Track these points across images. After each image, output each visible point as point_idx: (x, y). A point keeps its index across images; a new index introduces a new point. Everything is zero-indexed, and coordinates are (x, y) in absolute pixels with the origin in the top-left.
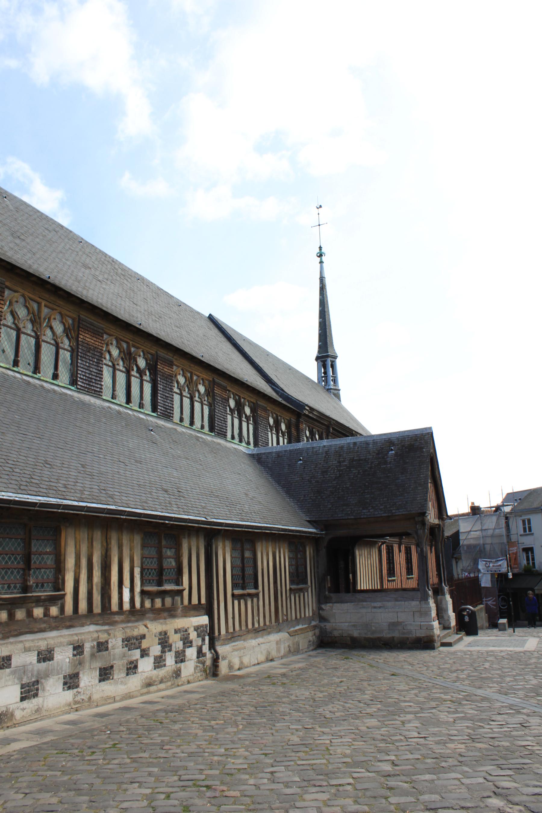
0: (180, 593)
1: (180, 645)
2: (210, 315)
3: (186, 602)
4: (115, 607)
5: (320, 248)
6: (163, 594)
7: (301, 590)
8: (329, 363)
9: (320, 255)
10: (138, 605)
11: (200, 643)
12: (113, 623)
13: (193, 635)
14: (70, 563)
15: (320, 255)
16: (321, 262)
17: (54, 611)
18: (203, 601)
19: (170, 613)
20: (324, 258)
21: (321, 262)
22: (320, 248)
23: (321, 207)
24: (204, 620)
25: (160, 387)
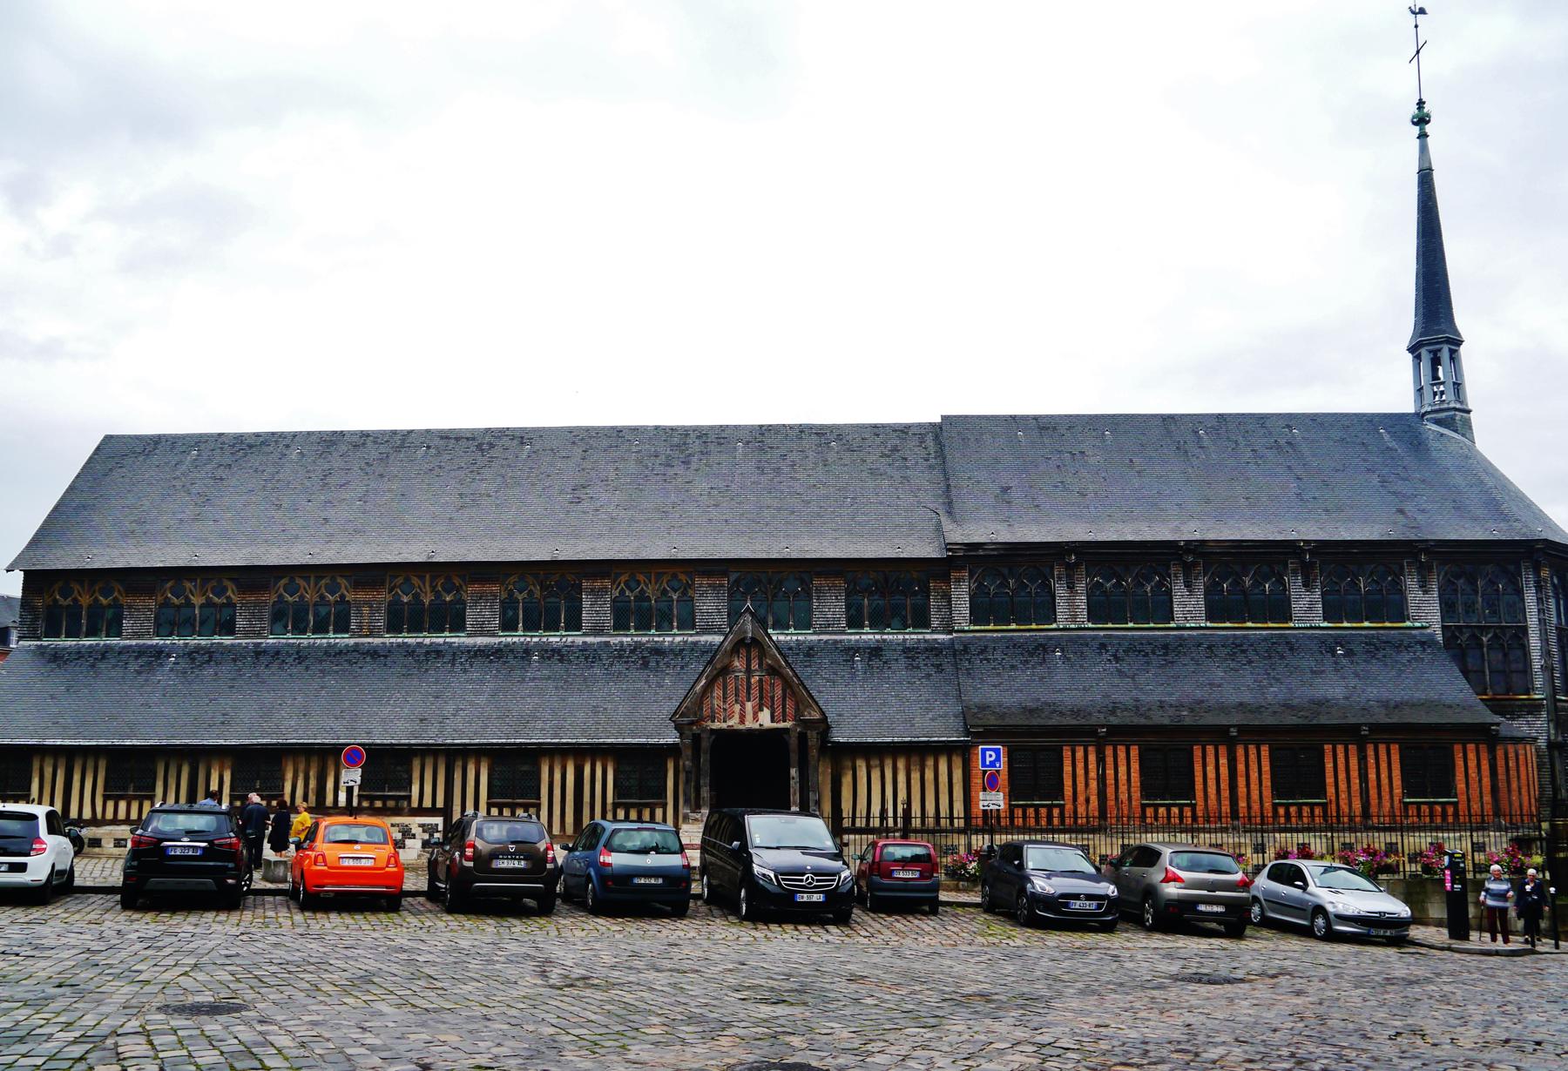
0: (409, 798)
1: (399, 836)
2: (943, 417)
3: (415, 804)
4: (329, 801)
5: (1421, 104)
6: (384, 799)
7: (646, 805)
8: (1445, 355)
9: (1421, 120)
10: (355, 803)
11: (426, 836)
12: (329, 815)
13: (416, 830)
14: (289, 775)
15: (1421, 120)
16: (1423, 136)
17: (274, 803)
18: (440, 804)
19: (397, 812)
20: (1428, 128)
21: (1423, 136)
22: (1421, 104)
23: (1422, 11)
24: (439, 821)
25: (586, 604)
